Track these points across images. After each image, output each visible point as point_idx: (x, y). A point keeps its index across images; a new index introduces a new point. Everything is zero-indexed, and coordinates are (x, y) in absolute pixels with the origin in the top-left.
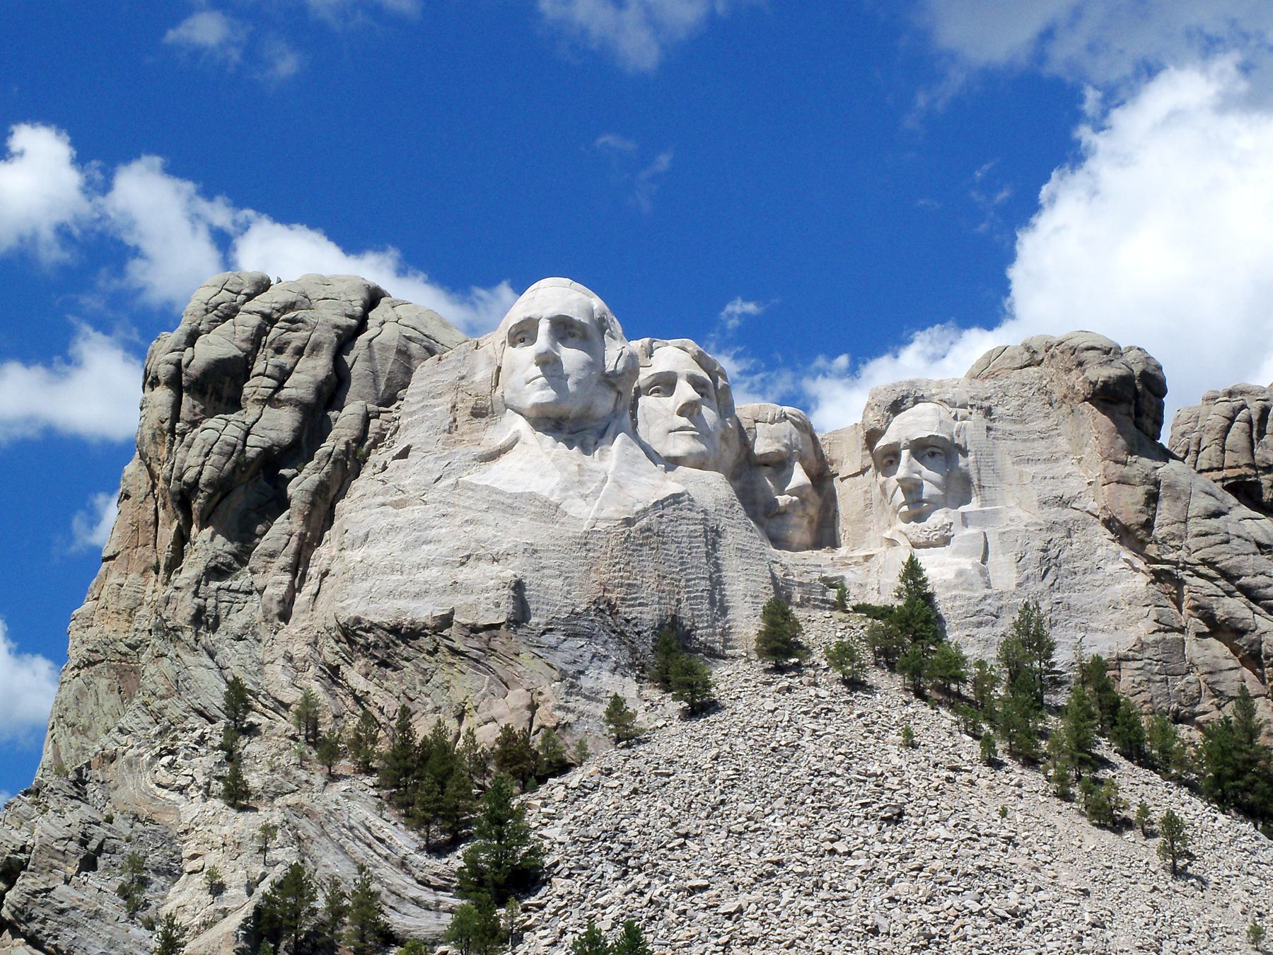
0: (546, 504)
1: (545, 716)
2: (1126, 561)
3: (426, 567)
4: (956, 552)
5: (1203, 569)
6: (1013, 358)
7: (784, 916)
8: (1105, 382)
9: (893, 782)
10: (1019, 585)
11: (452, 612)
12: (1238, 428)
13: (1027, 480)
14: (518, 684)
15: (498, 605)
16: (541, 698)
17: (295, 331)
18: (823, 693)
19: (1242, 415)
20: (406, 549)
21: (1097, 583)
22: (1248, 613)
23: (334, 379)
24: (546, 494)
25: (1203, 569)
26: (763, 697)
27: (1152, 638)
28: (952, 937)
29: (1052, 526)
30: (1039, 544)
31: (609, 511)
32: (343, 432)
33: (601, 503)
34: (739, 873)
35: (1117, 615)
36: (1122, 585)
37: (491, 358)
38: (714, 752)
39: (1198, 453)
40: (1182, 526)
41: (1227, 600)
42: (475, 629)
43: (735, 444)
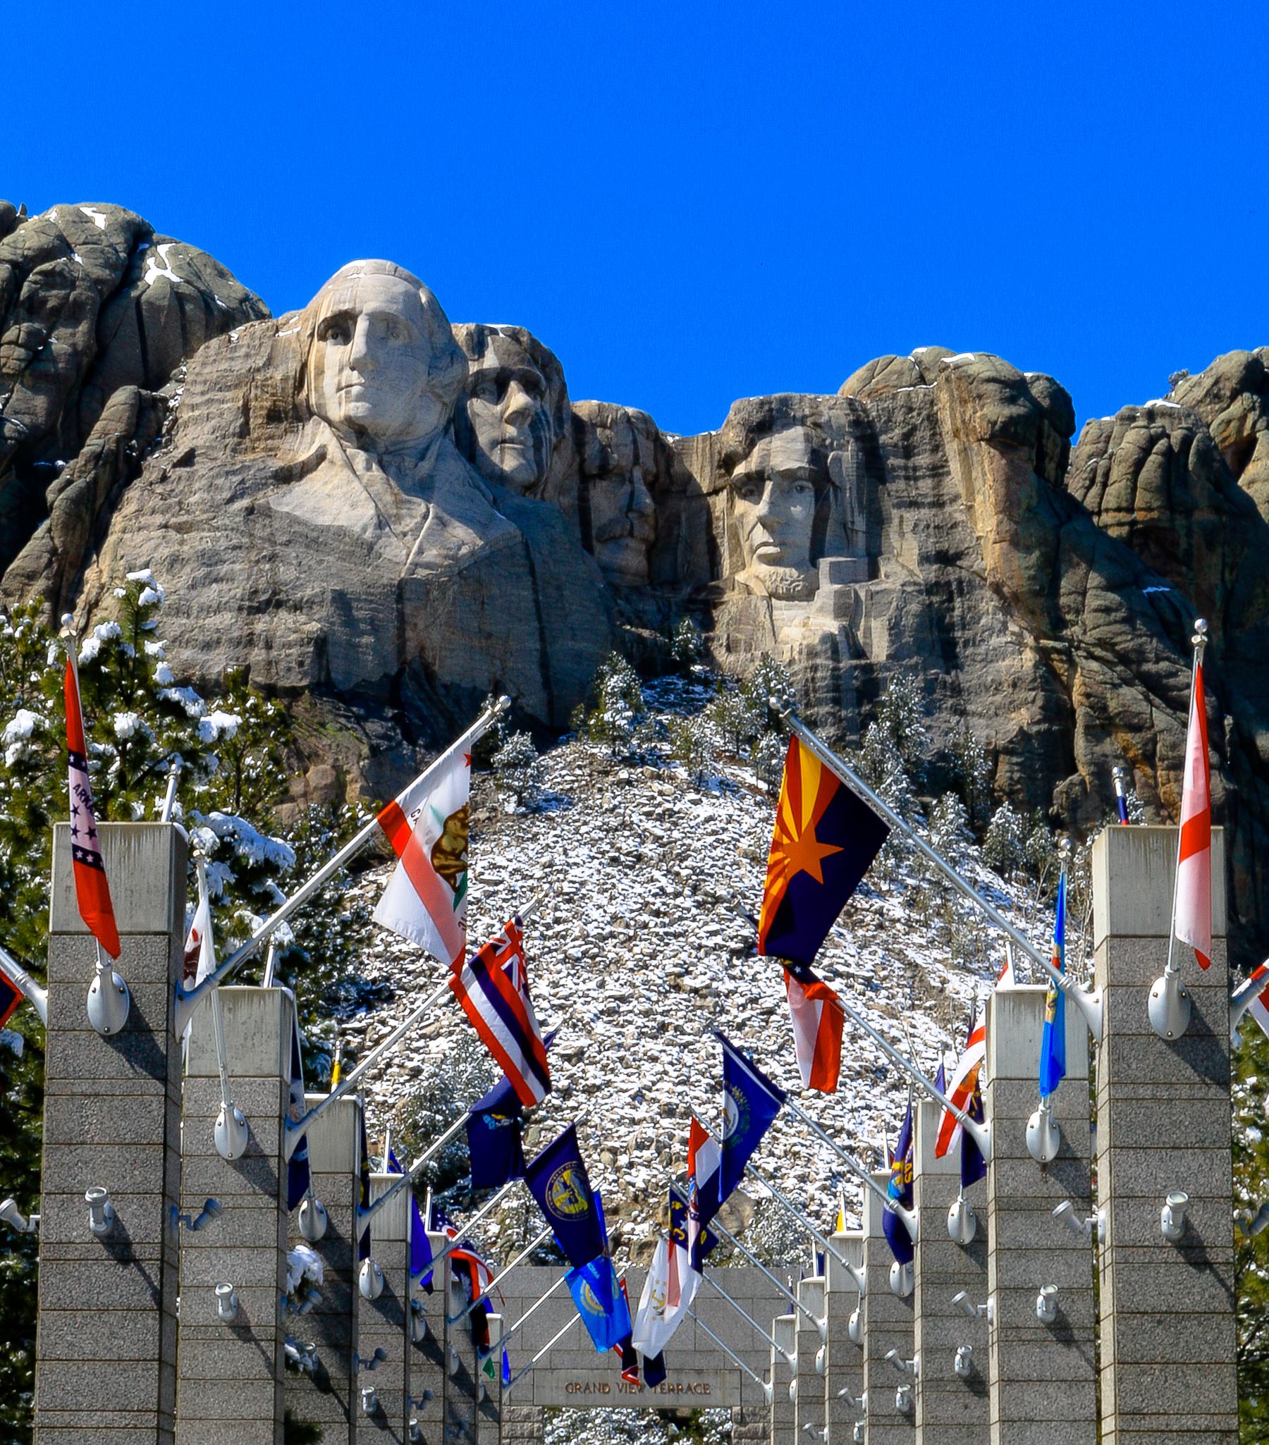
0: (359, 542)
2: (1013, 633)
3: (218, 610)
4: (821, 610)
5: (1098, 652)
6: (901, 373)
8: (1004, 423)
10: (889, 657)
12: (1153, 460)
13: (908, 527)
14: (323, 762)
15: (301, 664)
16: (349, 777)
17: (53, 288)
19: (1161, 445)
20: (193, 587)
21: (979, 658)
22: (1144, 707)
23: (95, 349)
24: (357, 529)
25: (1098, 652)
26: (600, 790)
27: (1035, 729)
29: (931, 589)
30: (914, 607)
31: (432, 554)
32: (112, 425)
33: (421, 542)
35: (998, 698)
36: (1007, 662)
39: (1105, 485)
40: (1080, 599)
41: (1125, 690)
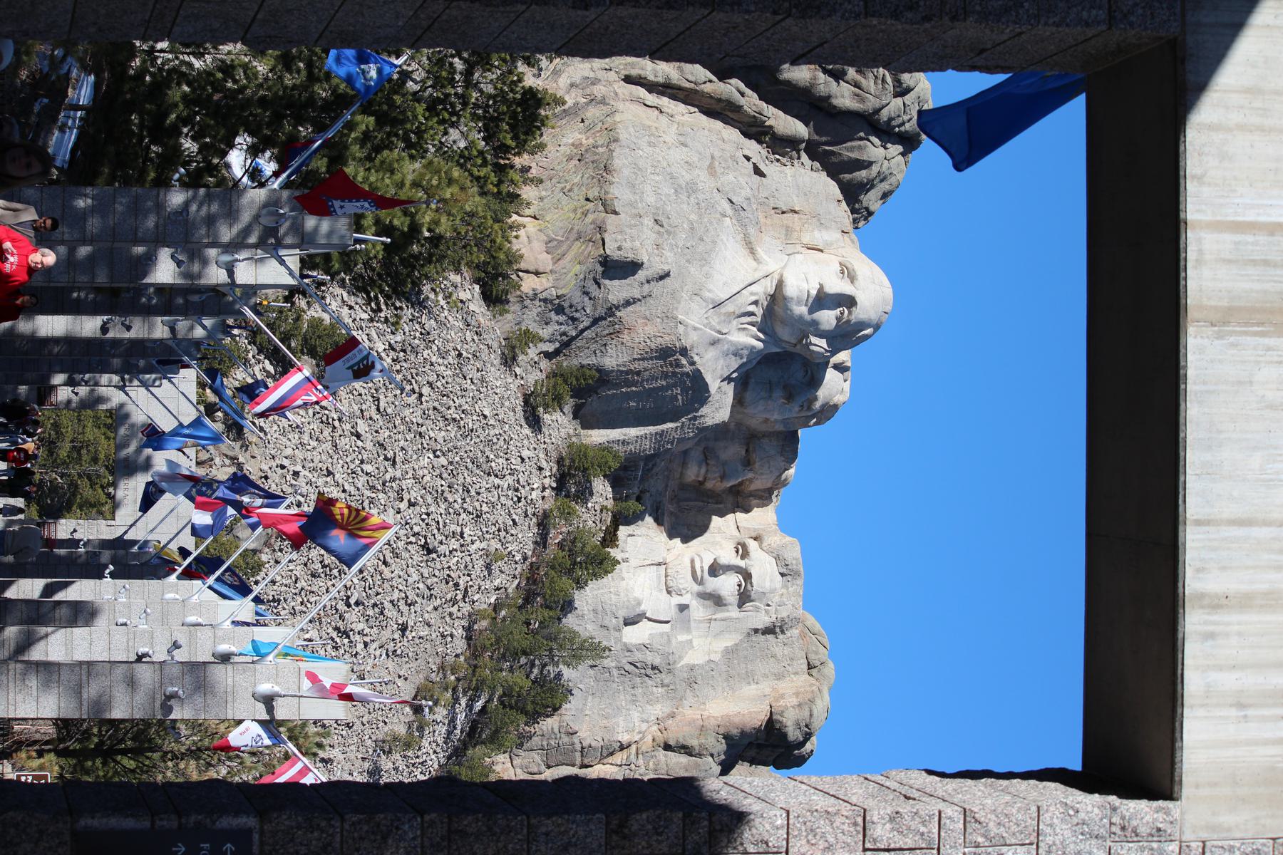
1: (529, 284)
6: (816, 653)
7: (352, 466)
9: (454, 544)
10: (625, 644)
11: (616, 213)
15: (620, 248)
18: (534, 495)
27: (576, 741)
28: (330, 583)
30: (657, 661)
34: (387, 433)
37: (832, 244)
38: (486, 413)
42: (601, 229)
43: (763, 428)
